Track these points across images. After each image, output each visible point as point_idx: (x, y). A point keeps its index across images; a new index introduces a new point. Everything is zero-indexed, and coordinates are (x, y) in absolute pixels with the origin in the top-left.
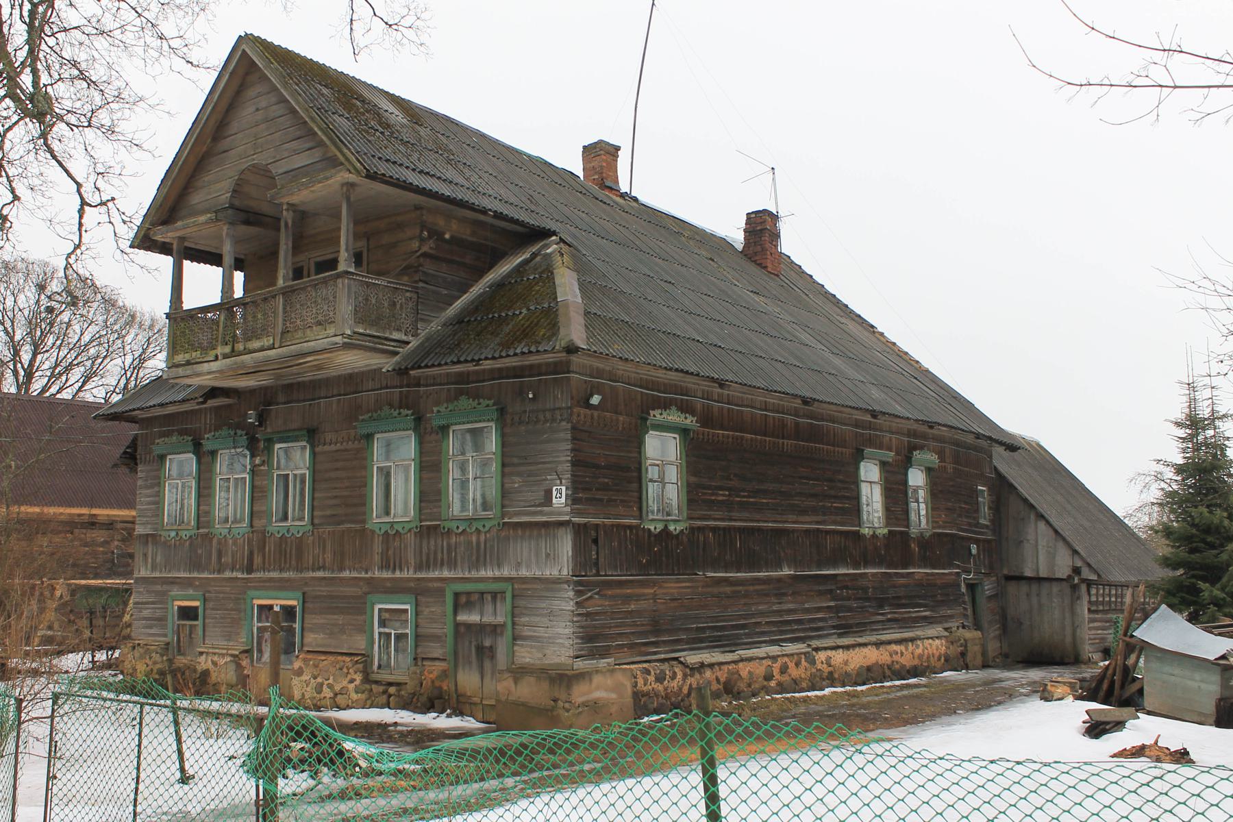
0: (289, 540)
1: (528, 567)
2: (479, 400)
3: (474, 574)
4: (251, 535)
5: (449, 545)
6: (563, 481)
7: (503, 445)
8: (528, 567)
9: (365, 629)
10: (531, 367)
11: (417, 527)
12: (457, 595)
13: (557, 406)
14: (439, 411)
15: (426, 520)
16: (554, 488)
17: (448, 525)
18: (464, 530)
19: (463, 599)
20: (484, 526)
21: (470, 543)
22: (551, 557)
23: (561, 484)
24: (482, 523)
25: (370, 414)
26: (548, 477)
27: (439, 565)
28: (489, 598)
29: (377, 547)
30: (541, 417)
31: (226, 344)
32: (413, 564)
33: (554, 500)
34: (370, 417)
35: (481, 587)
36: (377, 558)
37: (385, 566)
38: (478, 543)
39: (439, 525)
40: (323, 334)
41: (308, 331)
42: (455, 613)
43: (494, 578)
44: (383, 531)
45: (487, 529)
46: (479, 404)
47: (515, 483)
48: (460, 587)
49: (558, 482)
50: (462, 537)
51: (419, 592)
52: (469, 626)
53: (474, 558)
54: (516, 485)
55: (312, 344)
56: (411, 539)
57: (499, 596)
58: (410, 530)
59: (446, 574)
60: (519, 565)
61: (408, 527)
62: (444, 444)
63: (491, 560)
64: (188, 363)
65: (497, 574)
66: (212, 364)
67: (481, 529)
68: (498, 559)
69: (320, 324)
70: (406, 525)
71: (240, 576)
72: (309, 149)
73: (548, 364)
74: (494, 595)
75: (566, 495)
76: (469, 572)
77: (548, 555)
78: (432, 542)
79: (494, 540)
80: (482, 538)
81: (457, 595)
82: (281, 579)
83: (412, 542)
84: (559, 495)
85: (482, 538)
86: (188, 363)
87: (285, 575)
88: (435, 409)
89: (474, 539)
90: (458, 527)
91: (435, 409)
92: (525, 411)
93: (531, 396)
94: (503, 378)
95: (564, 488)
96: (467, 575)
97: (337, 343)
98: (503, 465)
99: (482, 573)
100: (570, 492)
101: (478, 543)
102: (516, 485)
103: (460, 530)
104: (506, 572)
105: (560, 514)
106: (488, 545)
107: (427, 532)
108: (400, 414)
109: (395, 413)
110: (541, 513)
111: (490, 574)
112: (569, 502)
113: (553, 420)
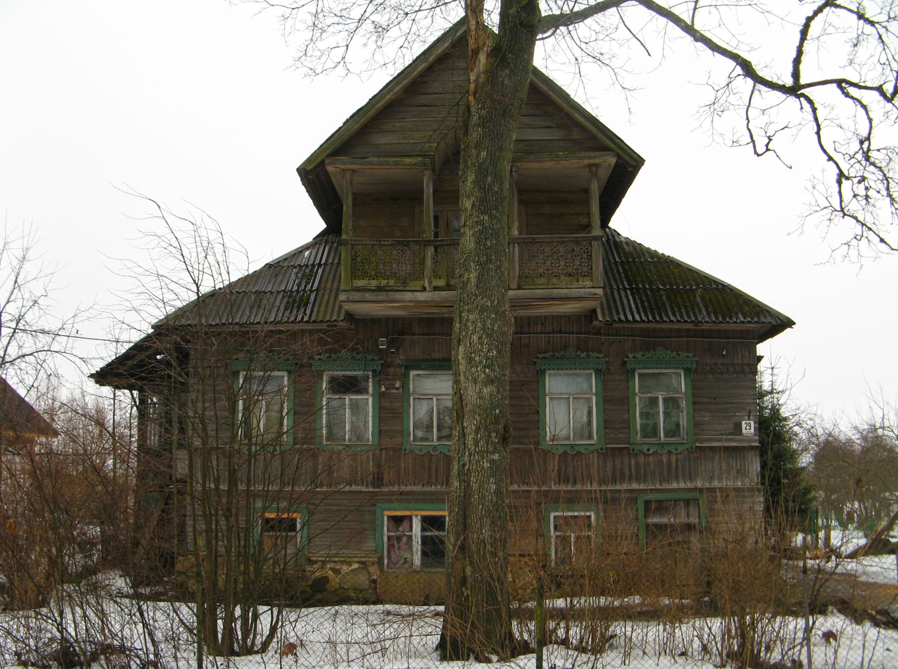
0: (434, 458)
1: (720, 479)
2: (677, 352)
3: (665, 486)
4: (378, 452)
5: (637, 464)
6: (751, 417)
7: (694, 388)
8: (720, 479)
9: (541, 534)
10: (718, 331)
11: (602, 449)
12: (647, 503)
13: (745, 362)
14: (634, 357)
15: (609, 444)
16: (743, 423)
17: (637, 448)
18: (654, 453)
19: (653, 506)
20: (676, 449)
21: (660, 462)
22: (742, 473)
23: (749, 419)
24: (675, 447)
25: (551, 353)
26: (737, 414)
27: (626, 480)
28: (682, 504)
29: (554, 465)
30: (731, 369)
31: (440, 278)
32: (597, 478)
33: (744, 431)
34: (553, 356)
35: (675, 496)
36: (554, 475)
37: (564, 478)
38: (669, 463)
39: (628, 448)
40: (575, 284)
41: (555, 280)
42: (646, 517)
43: (688, 489)
44: (560, 452)
45: (679, 451)
46: (679, 355)
47: (706, 417)
48: (651, 497)
49: (747, 418)
50: (651, 458)
51: (609, 501)
52: (660, 527)
53: (665, 473)
54: (707, 419)
55: (565, 291)
56: (595, 459)
57: (692, 502)
58: (592, 452)
59: (635, 486)
60: (712, 478)
61: (593, 448)
62: (631, 383)
63: (683, 476)
64: (380, 289)
65: (690, 485)
66: (419, 294)
67: (673, 451)
68: (690, 473)
69: (570, 275)
70: (589, 447)
71: (364, 489)
72: (545, 127)
73: (734, 331)
74: (687, 502)
75: (755, 428)
76: (661, 484)
77: (738, 471)
78: (618, 462)
79: (685, 460)
80: (673, 458)
81: (647, 503)
82: (423, 493)
83: (596, 461)
84: (748, 427)
85: (673, 458)
86: (380, 289)
87: (427, 489)
88: (631, 356)
89: (665, 459)
90: (648, 450)
91: (631, 356)
92: (716, 364)
93: (724, 353)
94: (691, 337)
95: (752, 423)
96: (658, 486)
97: (596, 294)
98: (694, 403)
99: (675, 485)
100: (757, 426)
101: (669, 463)
102: (707, 419)
103: (651, 452)
104: (699, 484)
105: (750, 441)
106: (679, 464)
107: (606, 453)
108: (588, 356)
109: (584, 355)
110: (732, 440)
111: (682, 485)
112: (757, 432)
113: (743, 372)
